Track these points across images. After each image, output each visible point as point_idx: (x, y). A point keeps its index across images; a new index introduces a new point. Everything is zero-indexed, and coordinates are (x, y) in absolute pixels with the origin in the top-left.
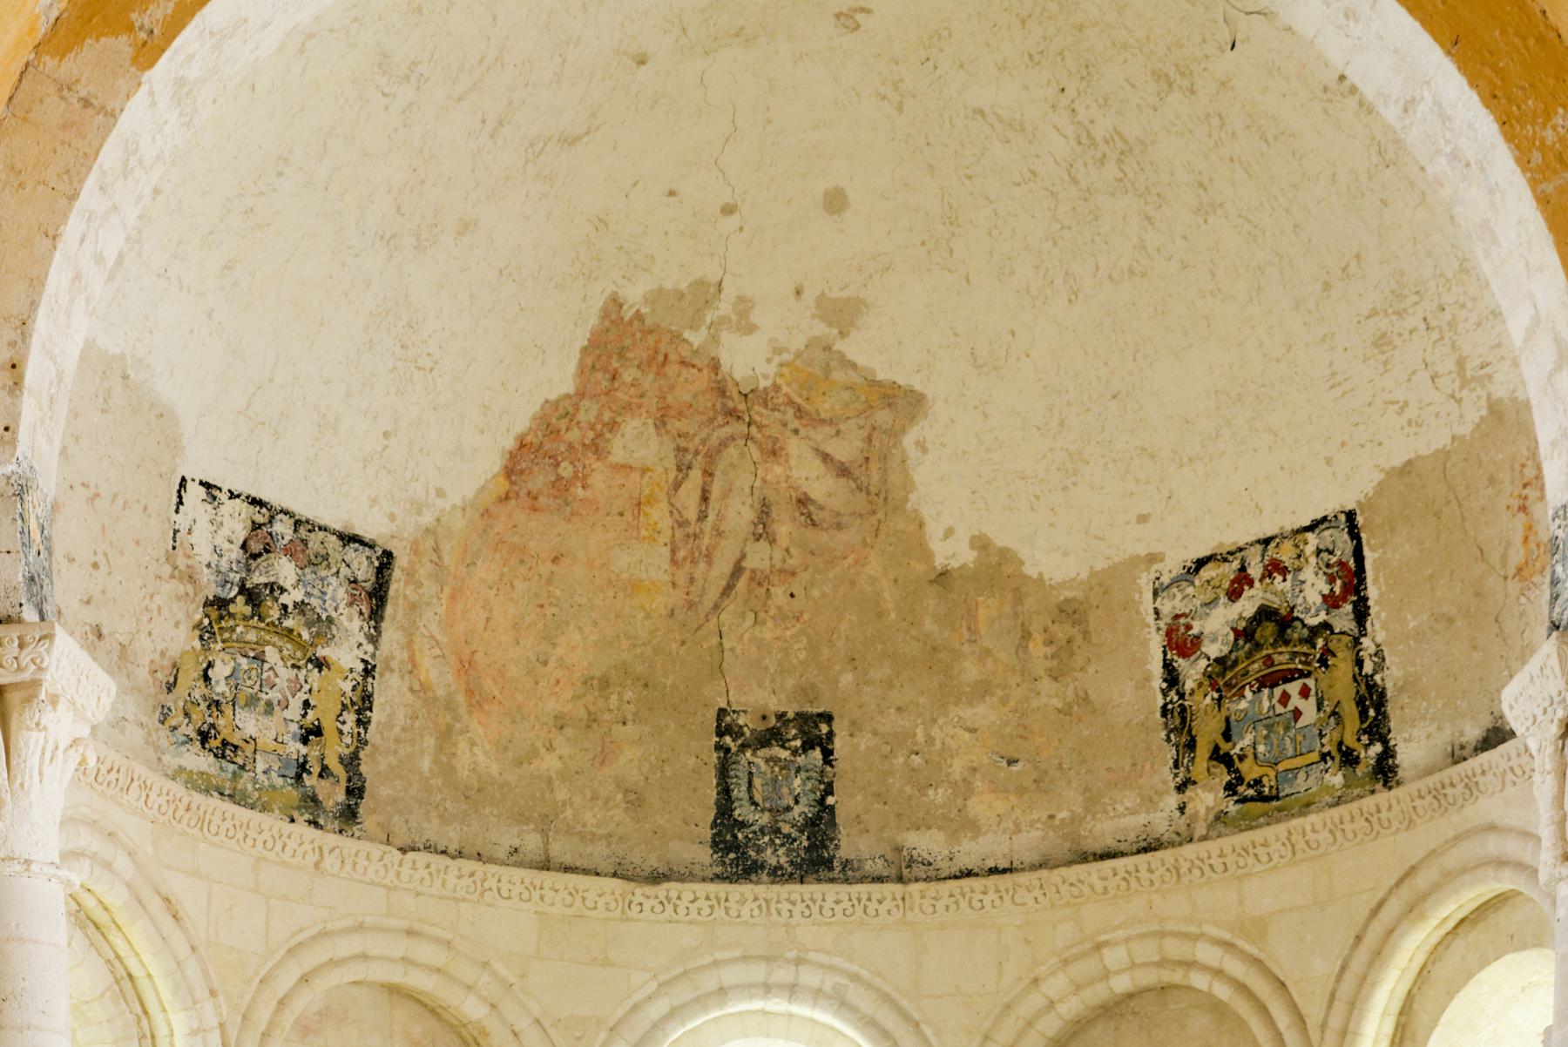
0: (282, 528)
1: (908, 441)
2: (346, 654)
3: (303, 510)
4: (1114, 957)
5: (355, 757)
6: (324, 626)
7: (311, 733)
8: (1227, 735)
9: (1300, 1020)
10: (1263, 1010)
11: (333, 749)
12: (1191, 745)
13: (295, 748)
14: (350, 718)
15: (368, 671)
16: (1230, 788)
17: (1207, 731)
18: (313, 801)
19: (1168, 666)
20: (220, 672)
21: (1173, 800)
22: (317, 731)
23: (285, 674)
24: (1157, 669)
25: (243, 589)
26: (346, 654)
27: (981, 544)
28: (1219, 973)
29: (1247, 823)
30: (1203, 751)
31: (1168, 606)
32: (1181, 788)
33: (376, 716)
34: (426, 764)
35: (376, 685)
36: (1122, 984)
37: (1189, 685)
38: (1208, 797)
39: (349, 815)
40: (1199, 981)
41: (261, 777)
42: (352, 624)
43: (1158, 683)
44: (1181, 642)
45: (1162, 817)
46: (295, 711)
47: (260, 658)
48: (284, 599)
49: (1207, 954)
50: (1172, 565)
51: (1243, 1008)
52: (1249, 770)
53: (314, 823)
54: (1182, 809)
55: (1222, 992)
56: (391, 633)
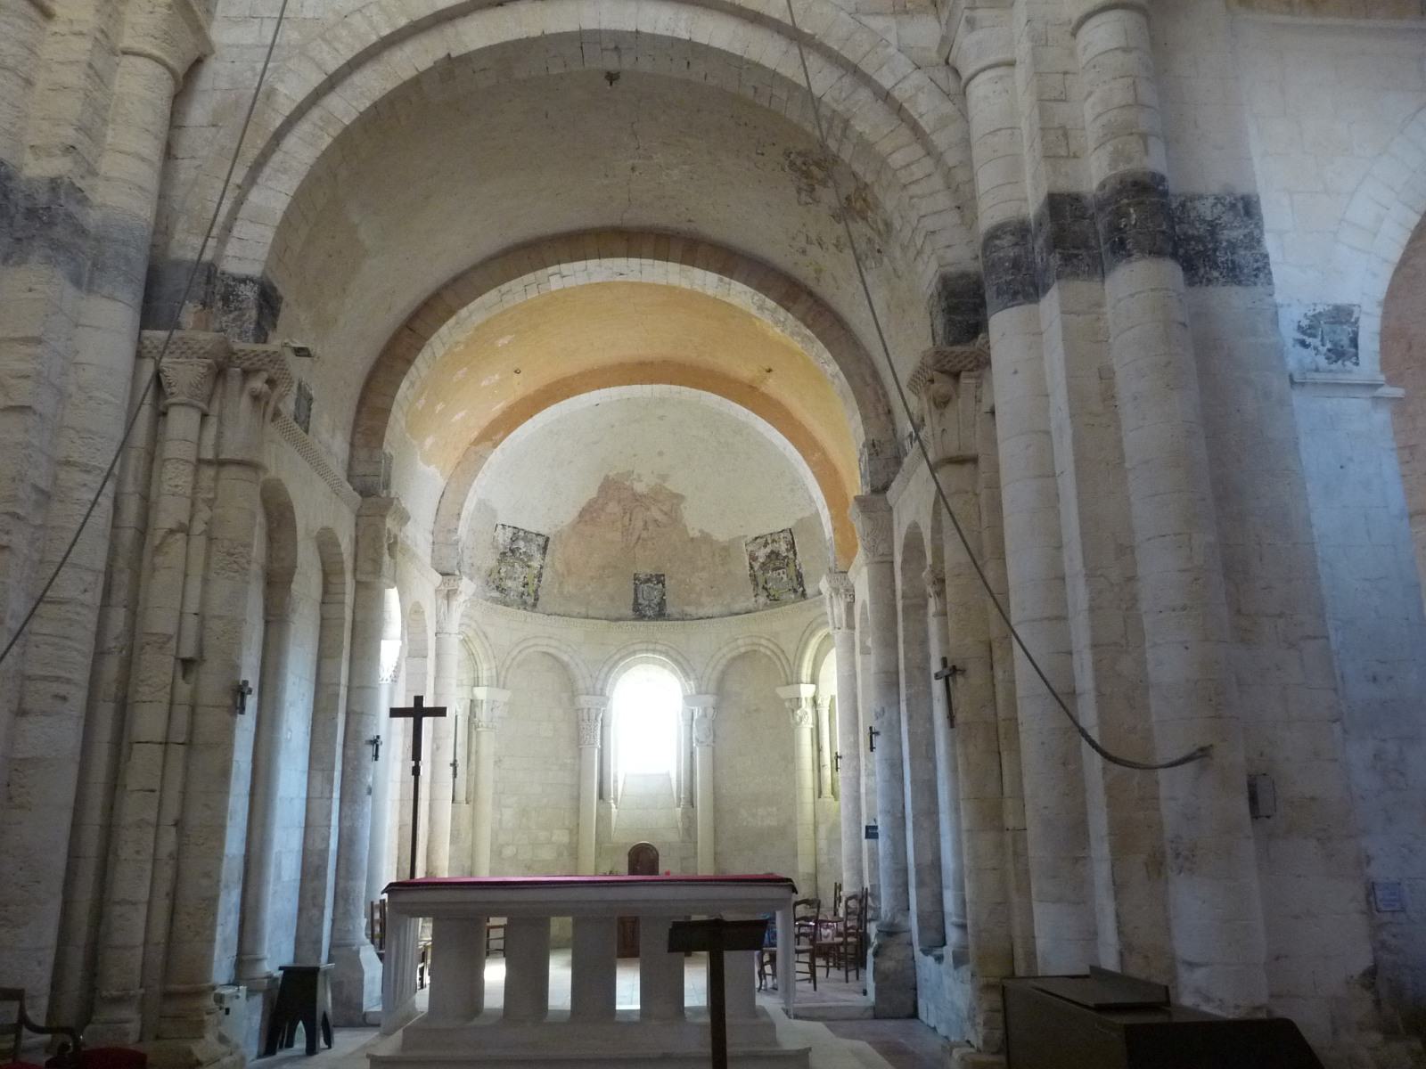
0: (521, 534)
1: (682, 506)
2: (536, 564)
3: (527, 529)
4: (740, 642)
5: (537, 590)
6: (530, 557)
7: (526, 585)
8: (766, 583)
9: (788, 660)
10: (779, 659)
11: (531, 589)
12: (757, 585)
13: (521, 589)
14: (536, 580)
15: (541, 568)
16: (768, 596)
17: (761, 581)
18: (525, 603)
19: (750, 564)
20: (503, 570)
21: (753, 599)
22: (527, 584)
23: (520, 569)
24: (747, 564)
25: (510, 549)
26: (536, 564)
27: (701, 531)
28: (767, 647)
29: (771, 607)
30: (760, 587)
31: (750, 549)
32: (755, 596)
33: (543, 579)
34: (556, 591)
35: (543, 571)
36: (743, 650)
37: (756, 569)
38: (762, 599)
39: (534, 605)
40: (762, 649)
41: (512, 598)
42: (538, 556)
43: (748, 568)
44: (753, 558)
45: (751, 604)
46: (522, 579)
47: (513, 566)
48: (521, 551)
49: (764, 642)
50: (749, 538)
51: (775, 658)
52: (772, 592)
53: (525, 609)
54: (756, 601)
55: (769, 653)
56: (548, 558)
